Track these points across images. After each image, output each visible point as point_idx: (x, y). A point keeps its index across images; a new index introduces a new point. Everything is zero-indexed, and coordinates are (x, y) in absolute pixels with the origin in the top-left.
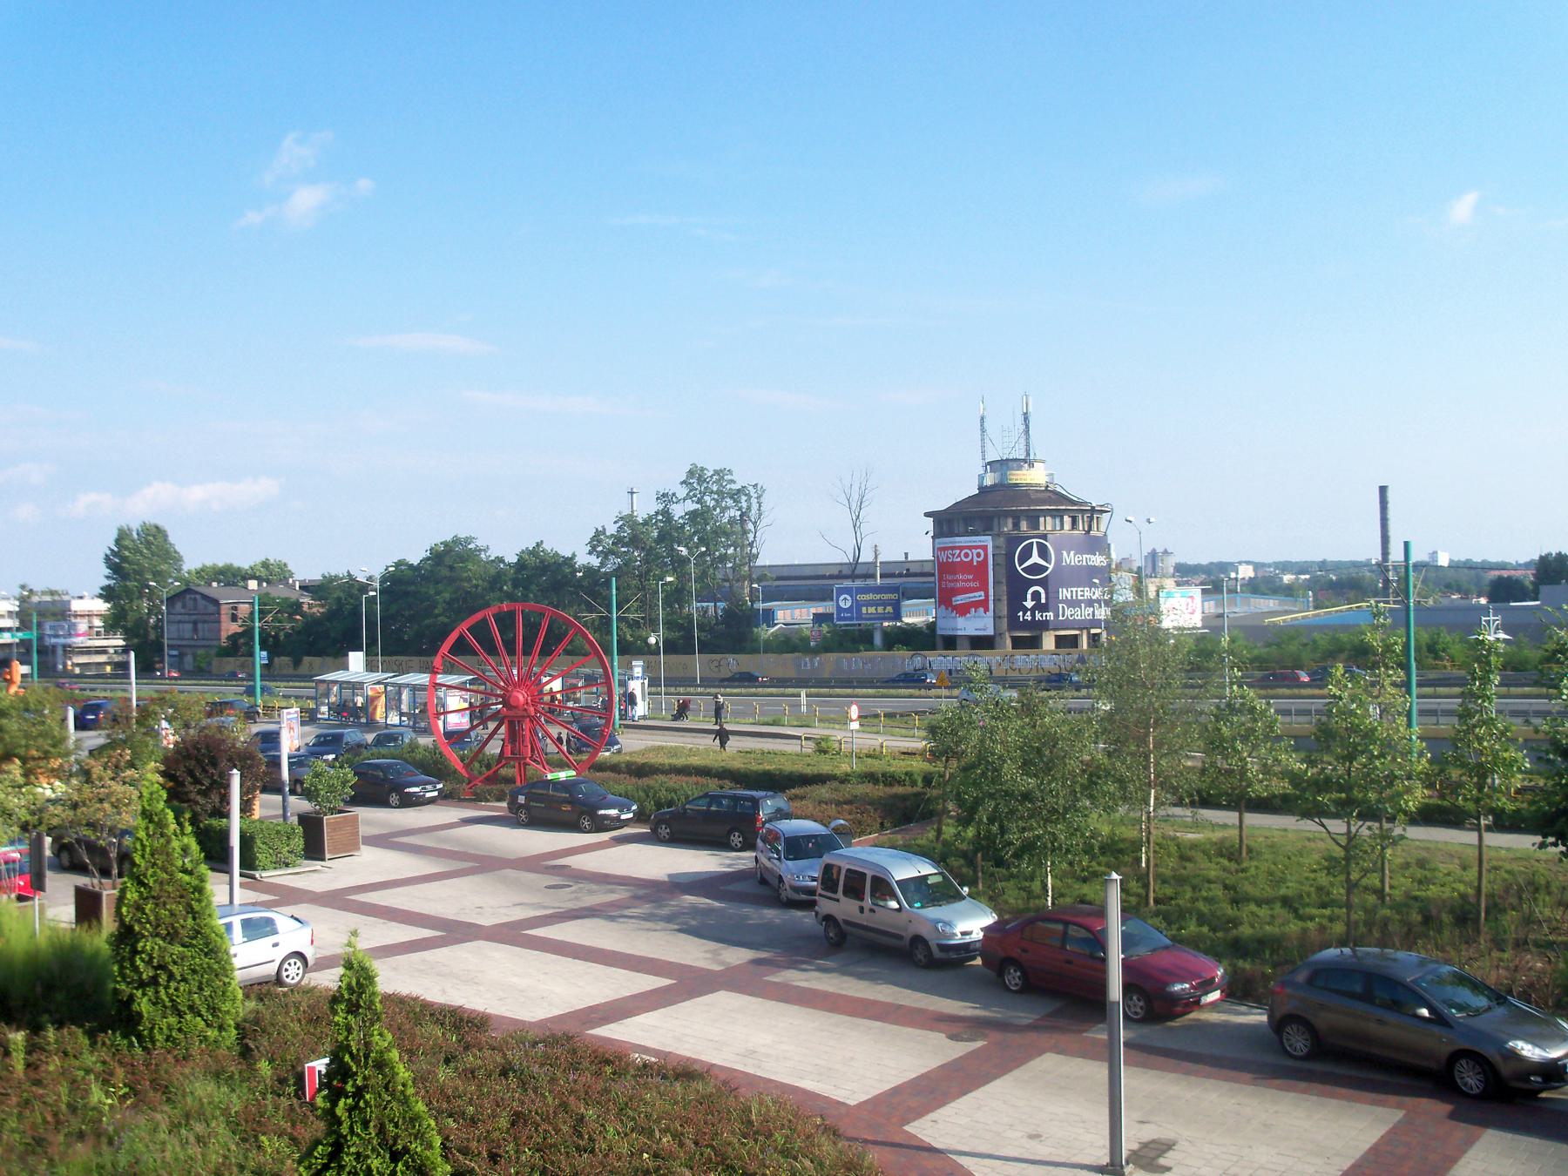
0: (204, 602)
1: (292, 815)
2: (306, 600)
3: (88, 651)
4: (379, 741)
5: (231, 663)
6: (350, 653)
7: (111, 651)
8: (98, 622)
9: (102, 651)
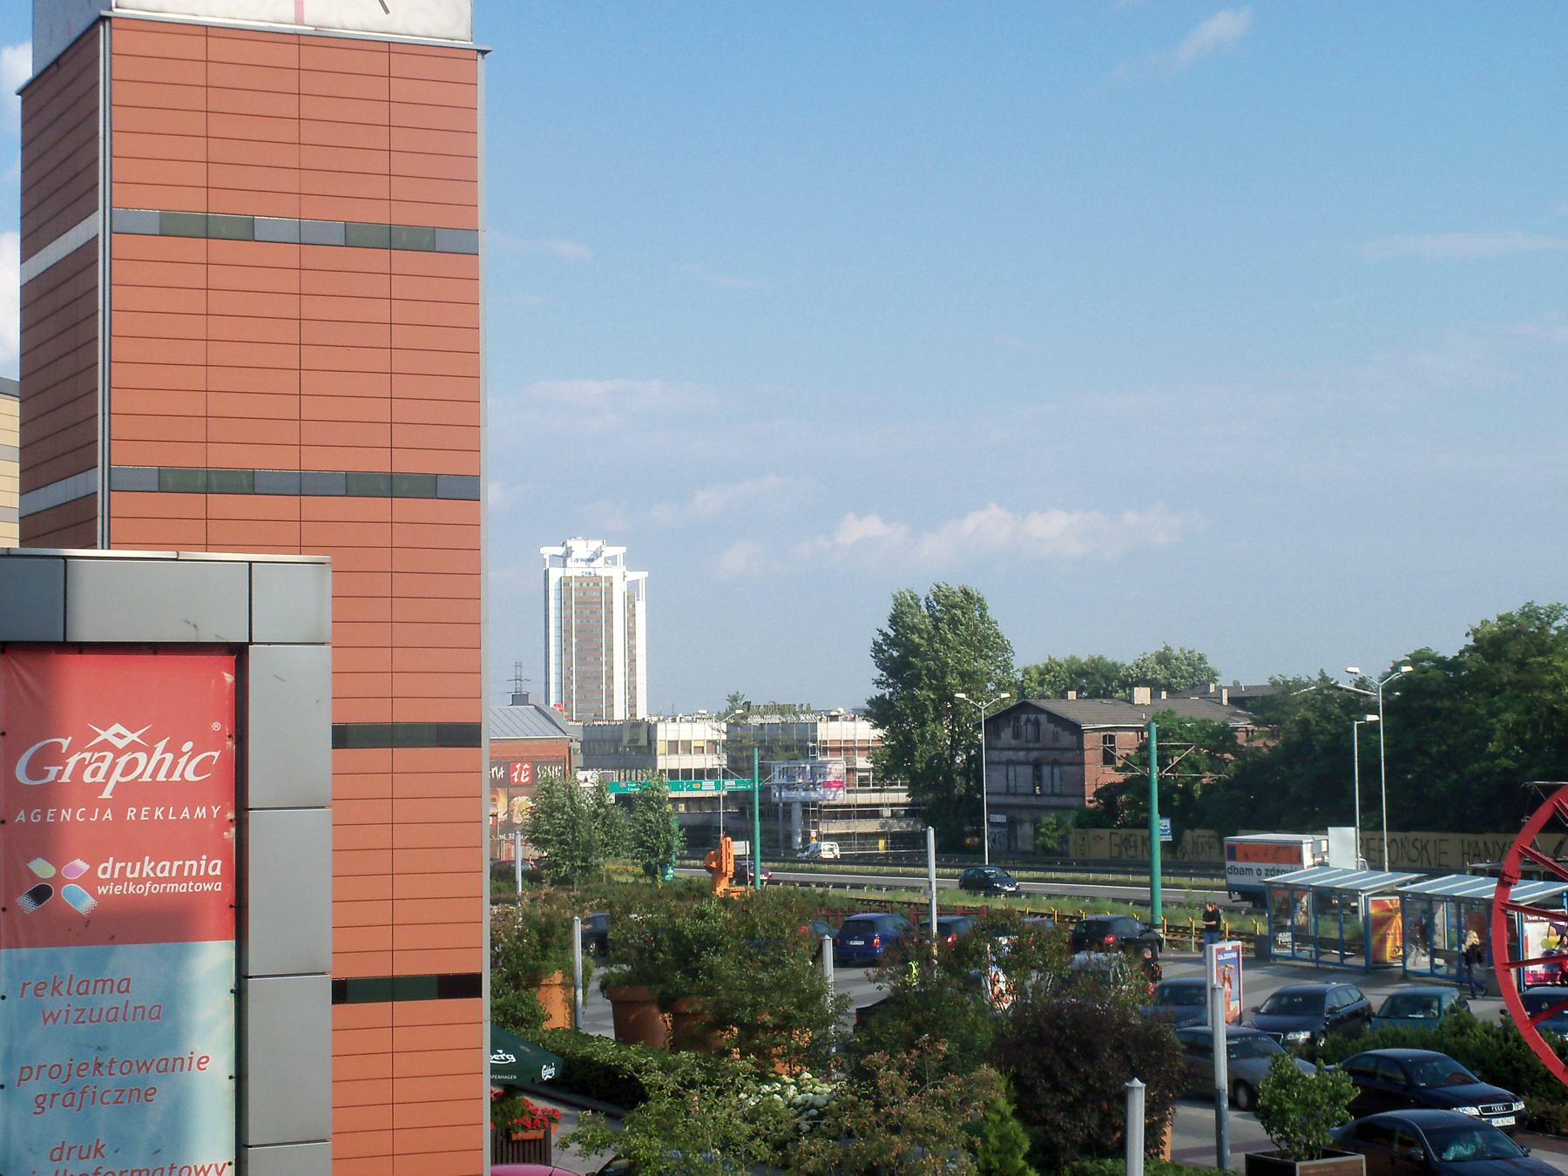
0: (1051, 726)
1: (1234, 1149)
2: (1242, 723)
3: (845, 812)
4: (1396, 1007)
5: (1103, 842)
6: (1329, 829)
7: (887, 812)
8: (862, 762)
9: (871, 812)
